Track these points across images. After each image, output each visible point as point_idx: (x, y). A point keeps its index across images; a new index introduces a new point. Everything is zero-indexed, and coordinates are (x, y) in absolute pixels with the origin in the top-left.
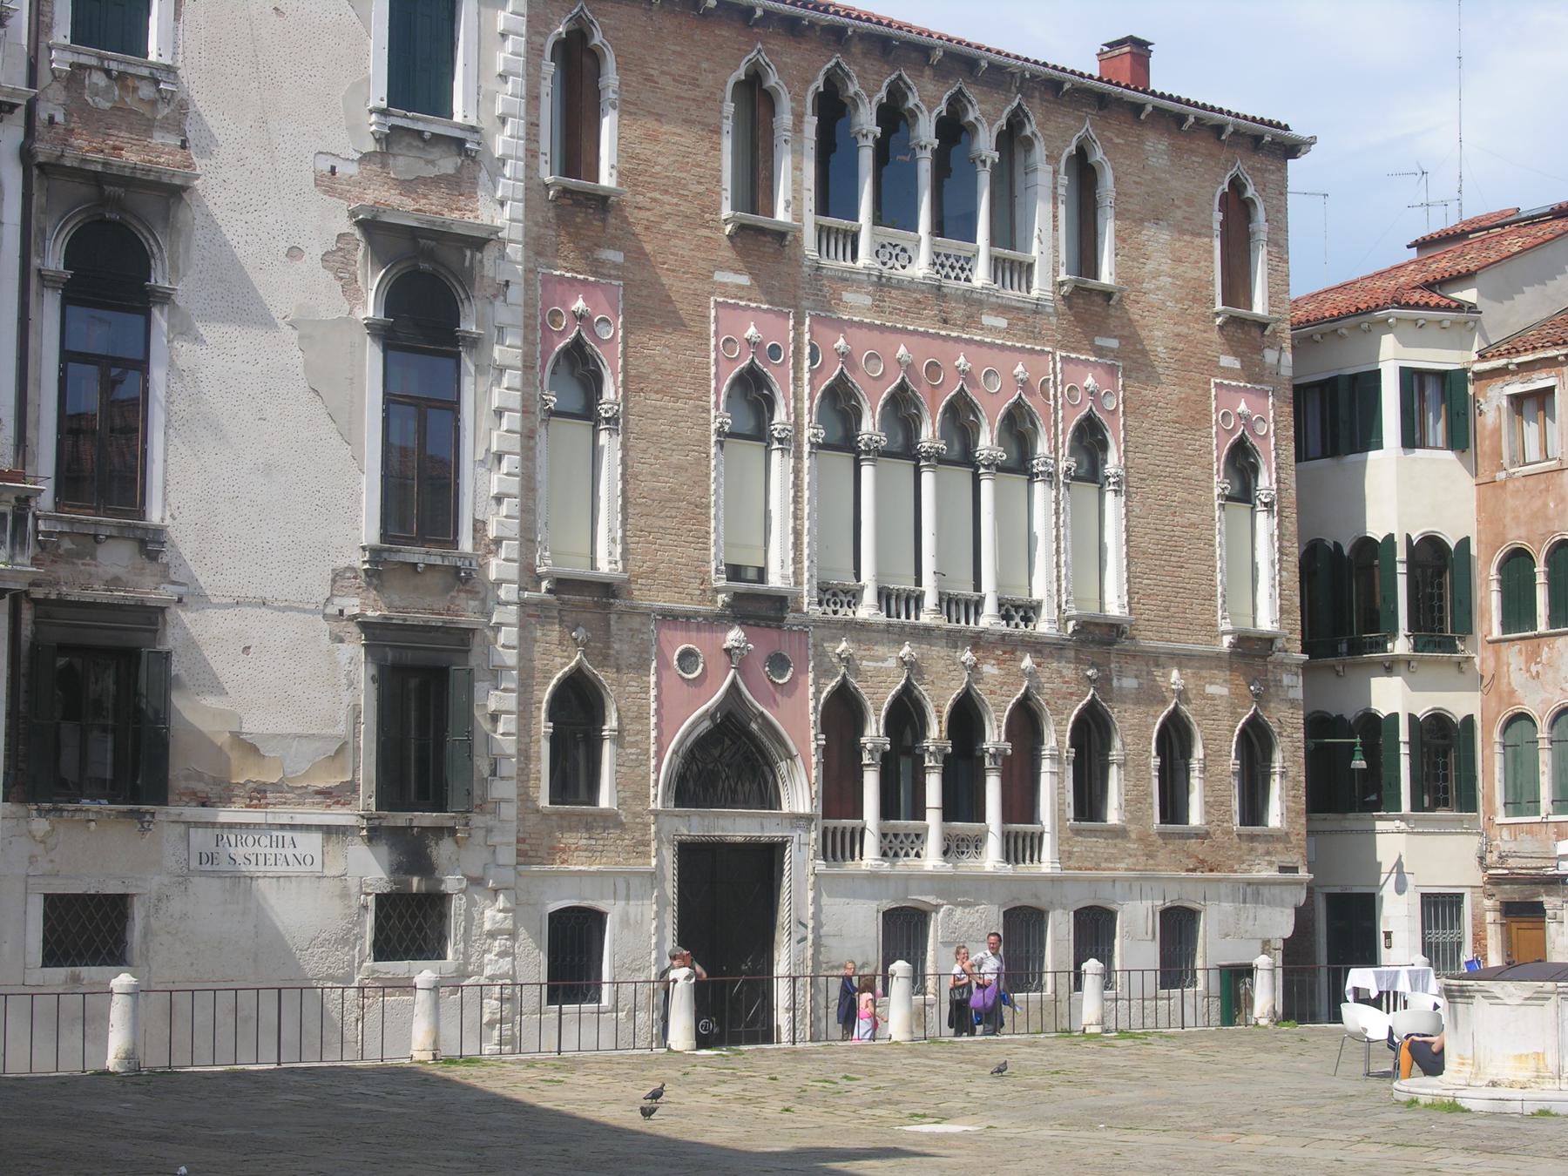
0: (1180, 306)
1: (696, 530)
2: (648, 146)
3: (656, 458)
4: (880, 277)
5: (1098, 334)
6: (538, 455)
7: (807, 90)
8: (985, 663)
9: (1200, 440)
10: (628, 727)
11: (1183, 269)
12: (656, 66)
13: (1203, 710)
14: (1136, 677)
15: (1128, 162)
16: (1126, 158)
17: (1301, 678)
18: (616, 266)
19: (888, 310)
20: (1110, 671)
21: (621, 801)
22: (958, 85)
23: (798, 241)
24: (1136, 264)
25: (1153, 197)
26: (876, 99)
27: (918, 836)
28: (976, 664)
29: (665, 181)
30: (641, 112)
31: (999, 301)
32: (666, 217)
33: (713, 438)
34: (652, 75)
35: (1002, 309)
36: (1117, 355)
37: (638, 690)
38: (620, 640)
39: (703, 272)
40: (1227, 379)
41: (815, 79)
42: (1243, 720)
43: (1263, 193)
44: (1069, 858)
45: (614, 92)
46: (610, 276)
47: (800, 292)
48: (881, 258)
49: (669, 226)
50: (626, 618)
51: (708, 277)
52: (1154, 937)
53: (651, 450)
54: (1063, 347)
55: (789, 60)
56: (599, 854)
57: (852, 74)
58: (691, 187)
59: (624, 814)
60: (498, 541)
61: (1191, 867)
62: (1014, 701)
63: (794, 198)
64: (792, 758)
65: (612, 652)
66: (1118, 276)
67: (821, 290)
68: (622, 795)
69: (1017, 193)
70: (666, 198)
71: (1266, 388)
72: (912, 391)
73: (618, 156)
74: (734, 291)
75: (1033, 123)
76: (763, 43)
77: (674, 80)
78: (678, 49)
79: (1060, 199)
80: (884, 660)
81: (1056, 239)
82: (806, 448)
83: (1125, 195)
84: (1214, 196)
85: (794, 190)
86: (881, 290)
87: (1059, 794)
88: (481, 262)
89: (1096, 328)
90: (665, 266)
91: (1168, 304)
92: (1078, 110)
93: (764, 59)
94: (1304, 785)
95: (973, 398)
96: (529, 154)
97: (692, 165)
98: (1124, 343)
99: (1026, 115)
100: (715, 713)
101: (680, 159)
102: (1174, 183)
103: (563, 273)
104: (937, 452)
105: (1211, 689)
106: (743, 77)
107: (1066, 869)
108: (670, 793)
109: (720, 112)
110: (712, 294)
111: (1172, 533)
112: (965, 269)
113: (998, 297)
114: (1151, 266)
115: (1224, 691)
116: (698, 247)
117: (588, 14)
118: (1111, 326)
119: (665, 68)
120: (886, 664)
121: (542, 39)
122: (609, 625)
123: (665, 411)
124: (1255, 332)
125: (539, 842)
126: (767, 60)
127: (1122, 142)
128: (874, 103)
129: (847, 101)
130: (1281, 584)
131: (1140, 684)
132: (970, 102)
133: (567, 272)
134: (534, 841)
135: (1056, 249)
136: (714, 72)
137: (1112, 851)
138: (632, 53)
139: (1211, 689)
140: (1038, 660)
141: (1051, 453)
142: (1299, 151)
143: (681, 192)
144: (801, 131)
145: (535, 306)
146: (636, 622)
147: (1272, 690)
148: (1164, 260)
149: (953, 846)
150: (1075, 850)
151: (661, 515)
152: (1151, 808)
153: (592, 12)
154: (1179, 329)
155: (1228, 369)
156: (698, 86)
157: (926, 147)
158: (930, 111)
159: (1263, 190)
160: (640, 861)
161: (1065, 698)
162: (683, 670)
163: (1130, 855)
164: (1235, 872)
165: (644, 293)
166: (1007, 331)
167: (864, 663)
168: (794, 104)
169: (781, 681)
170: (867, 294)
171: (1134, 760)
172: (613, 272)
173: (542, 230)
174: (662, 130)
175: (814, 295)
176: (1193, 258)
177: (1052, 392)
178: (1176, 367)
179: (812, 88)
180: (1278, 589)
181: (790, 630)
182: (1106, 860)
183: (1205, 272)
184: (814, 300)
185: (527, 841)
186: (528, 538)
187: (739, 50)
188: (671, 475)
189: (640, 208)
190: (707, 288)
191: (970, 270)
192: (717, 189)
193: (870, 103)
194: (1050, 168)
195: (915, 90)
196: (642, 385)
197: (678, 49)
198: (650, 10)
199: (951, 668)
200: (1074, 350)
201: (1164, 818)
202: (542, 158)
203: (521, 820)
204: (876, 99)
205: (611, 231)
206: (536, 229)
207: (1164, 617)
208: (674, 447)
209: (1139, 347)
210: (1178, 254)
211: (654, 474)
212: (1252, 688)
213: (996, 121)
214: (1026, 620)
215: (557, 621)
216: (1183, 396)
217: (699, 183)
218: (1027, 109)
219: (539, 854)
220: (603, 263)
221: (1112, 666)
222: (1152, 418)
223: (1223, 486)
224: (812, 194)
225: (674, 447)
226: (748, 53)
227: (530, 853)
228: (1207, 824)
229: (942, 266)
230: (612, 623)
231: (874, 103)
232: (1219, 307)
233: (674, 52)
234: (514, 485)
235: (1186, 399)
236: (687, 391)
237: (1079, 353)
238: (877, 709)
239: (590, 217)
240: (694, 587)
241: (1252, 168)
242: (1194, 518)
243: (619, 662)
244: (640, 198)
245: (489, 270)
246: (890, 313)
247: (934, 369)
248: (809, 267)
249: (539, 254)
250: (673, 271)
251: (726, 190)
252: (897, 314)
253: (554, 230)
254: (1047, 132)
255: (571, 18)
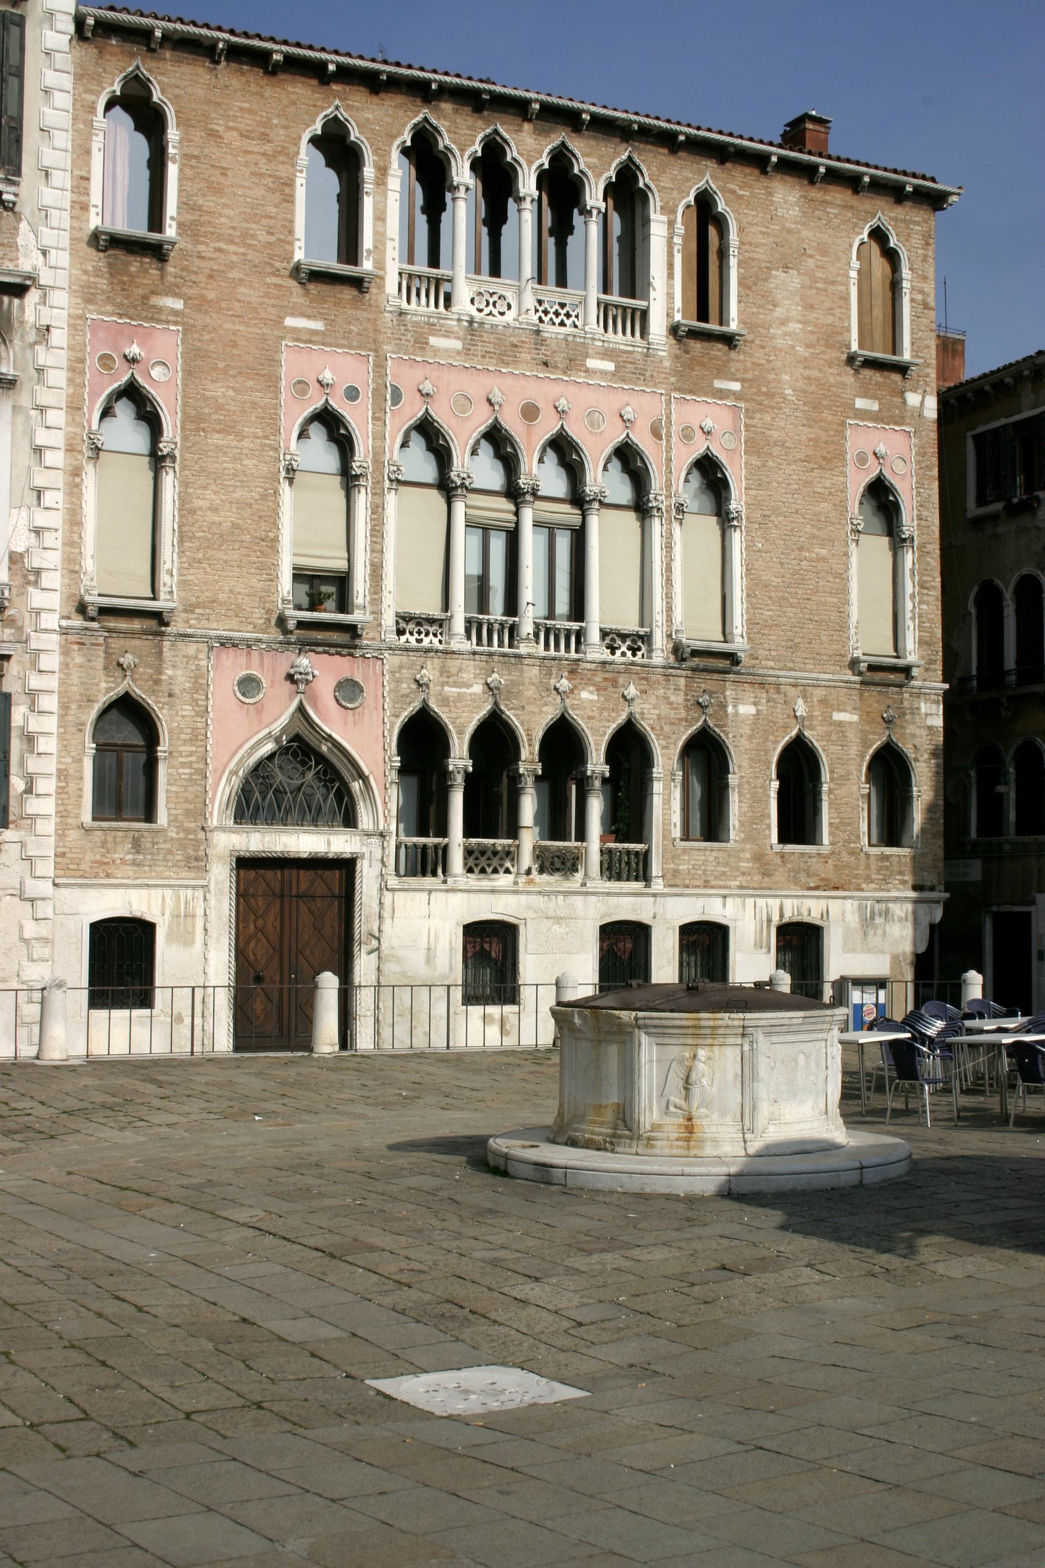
0: (813, 351)
1: (260, 562)
2: (212, 198)
3: (215, 493)
4: (471, 322)
5: (718, 376)
6: (84, 491)
7: (391, 145)
8: (583, 689)
9: (831, 479)
10: (181, 749)
11: (815, 315)
12: (221, 122)
13: (830, 736)
14: (755, 704)
15: (754, 213)
16: (752, 210)
17: (941, 706)
18: (175, 313)
19: (480, 353)
20: (725, 698)
21: (171, 818)
22: (561, 139)
23: (381, 288)
24: (761, 311)
25: (782, 246)
26: (468, 153)
27: (508, 854)
28: (572, 691)
29: (231, 232)
30: (204, 166)
31: (606, 345)
32: (231, 266)
33: (283, 474)
34: (218, 131)
35: (607, 354)
36: (738, 396)
37: (193, 714)
38: (173, 666)
39: (273, 317)
40: (863, 420)
41: (400, 133)
42: (875, 747)
43: (908, 244)
44: (674, 876)
45: (174, 147)
46: (168, 322)
47: (381, 338)
48: (476, 305)
49: (234, 274)
50: (180, 645)
51: (279, 322)
52: (769, 951)
53: (213, 487)
54: (676, 389)
55: (371, 117)
56: (147, 868)
57: (442, 129)
58: (261, 238)
59: (175, 830)
60: (38, 572)
61: (812, 885)
62: (615, 726)
63: (375, 247)
64: (362, 776)
65: (164, 677)
66: (742, 321)
67: (404, 335)
68: (173, 812)
69: (637, 245)
70: (232, 248)
71: (907, 429)
72: (506, 430)
73: (178, 208)
74: (305, 337)
75: (646, 175)
76: (342, 100)
77: (241, 135)
78: (247, 105)
79: (676, 248)
80: (468, 686)
81: (670, 287)
82: (387, 484)
83: (750, 244)
84: (851, 246)
85: (375, 241)
86: (472, 335)
87: (664, 814)
88: (22, 309)
89: (715, 371)
90: (230, 313)
91: (798, 348)
92: (697, 163)
93: (343, 114)
94: (942, 808)
95: (575, 437)
96: (77, 207)
97: (262, 217)
98: (746, 385)
99: (638, 168)
100: (281, 736)
101: (248, 210)
102: (805, 233)
103: (115, 319)
104: (533, 489)
105: (838, 716)
106: (319, 132)
107: (670, 886)
108: (229, 812)
109: (293, 166)
110: (283, 338)
111: (798, 567)
112: (543, 312)
113: (603, 341)
114: (779, 312)
115: (855, 718)
116: (267, 295)
117: (145, 72)
118: (733, 370)
119: (231, 124)
120: (470, 690)
121: (93, 98)
122: (160, 653)
123: (228, 450)
124: (896, 377)
125: (81, 856)
126: (346, 115)
127: (748, 194)
128: (466, 157)
129: (441, 156)
130: (920, 616)
131: (758, 711)
132: (574, 155)
133: (120, 318)
134: (74, 856)
135: (670, 296)
136: (286, 127)
137: (724, 869)
138: (195, 110)
139: (838, 716)
140: (643, 687)
141: (662, 489)
142: (946, 201)
143: (248, 242)
144: (384, 184)
145: (83, 351)
146: (191, 649)
147: (908, 717)
148: (793, 307)
149: (547, 864)
150: (681, 867)
151: (223, 548)
152: (769, 827)
153: (149, 70)
154: (807, 373)
155: (866, 411)
156: (269, 141)
157: (524, 198)
158: (530, 163)
159: (907, 240)
160: (193, 875)
161: (673, 724)
162: (243, 694)
163: (744, 874)
164: (862, 890)
165: (207, 338)
166: (614, 375)
167: (446, 688)
168: (376, 158)
169: (350, 706)
170: (458, 338)
171: (748, 782)
172: (171, 318)
173: (92, 279)
174: (228, 183)
175: (395, 339)
176: (827, 305)
177: (664, 432)
178: (806, 408)
179: (398, 142)
180: (917, 621)
181: (363, 656)
182: (716, 878)
183: (841, 319)
184: (397, 344)
185: (68, 855)
186: (72, 569)
187: (314, 106)
188: (234, 510)
189: (203, 258)
190: (277, 333)
191: (577, 316)
192: (289, 238)
193: (462, 156)
194: (665, 218)
195: (512, 144)
196: (202, 425)
197: (247, 105)
198: (215, 69)
199: (543, 694)
200: (691, 392)
201: (786, 836)
202: (93, 211)
203: (61, 834)
204: (468, 153)
205: (170, 279)
206: (85, 277)
207: (788, 647)
208: (238, 484)
209: (764, 389)
210: (809, 301)
211: (215, 510)
212: (885, 715)
213: (602, 174)
214: (634, 651)
215: (102, 648)
216: (813, 436)
217: (271, 234)
218: (638, 161)
219: (81, 868)
220: (160, 310)
221: (728, 693)
222: (777, 457)
223: (855, 522)
224: (396, 244)
225: (238, 484)
226: (323, 109)
227: (71, 867)
228: (831, 844)
229: (546, 312)
230: (165, 650)
231: (466, 157)
232: (855, 347)
233: (241, 109)
234: (54, 519)
235: (816, 440)
236: (252, 430)
237: (694, 394)
238: (460, 733)
239: (147, 266)
240: (258, 616)
241: (896, 219)
242: (824, 552)
243: (171, 687)
244: (201, 248)
245: (30, 316)
246: (483, 357)
247: (530, 412)
248: (391, 312)
249: (88, 301)
250: (239, 316)
251: (299, 240)
252: (490, 358)
253: (106, 279)
254: (662, 184)
255: (125, 77)
